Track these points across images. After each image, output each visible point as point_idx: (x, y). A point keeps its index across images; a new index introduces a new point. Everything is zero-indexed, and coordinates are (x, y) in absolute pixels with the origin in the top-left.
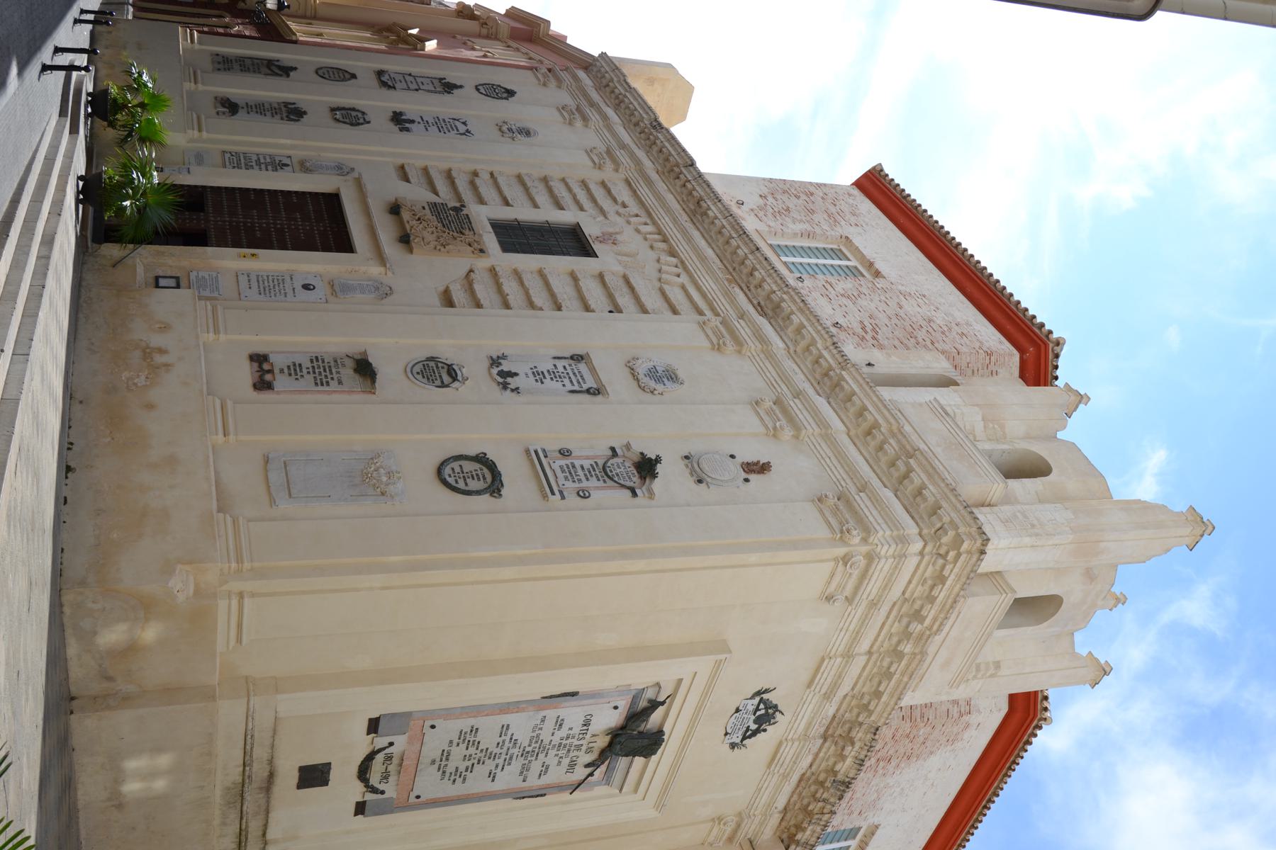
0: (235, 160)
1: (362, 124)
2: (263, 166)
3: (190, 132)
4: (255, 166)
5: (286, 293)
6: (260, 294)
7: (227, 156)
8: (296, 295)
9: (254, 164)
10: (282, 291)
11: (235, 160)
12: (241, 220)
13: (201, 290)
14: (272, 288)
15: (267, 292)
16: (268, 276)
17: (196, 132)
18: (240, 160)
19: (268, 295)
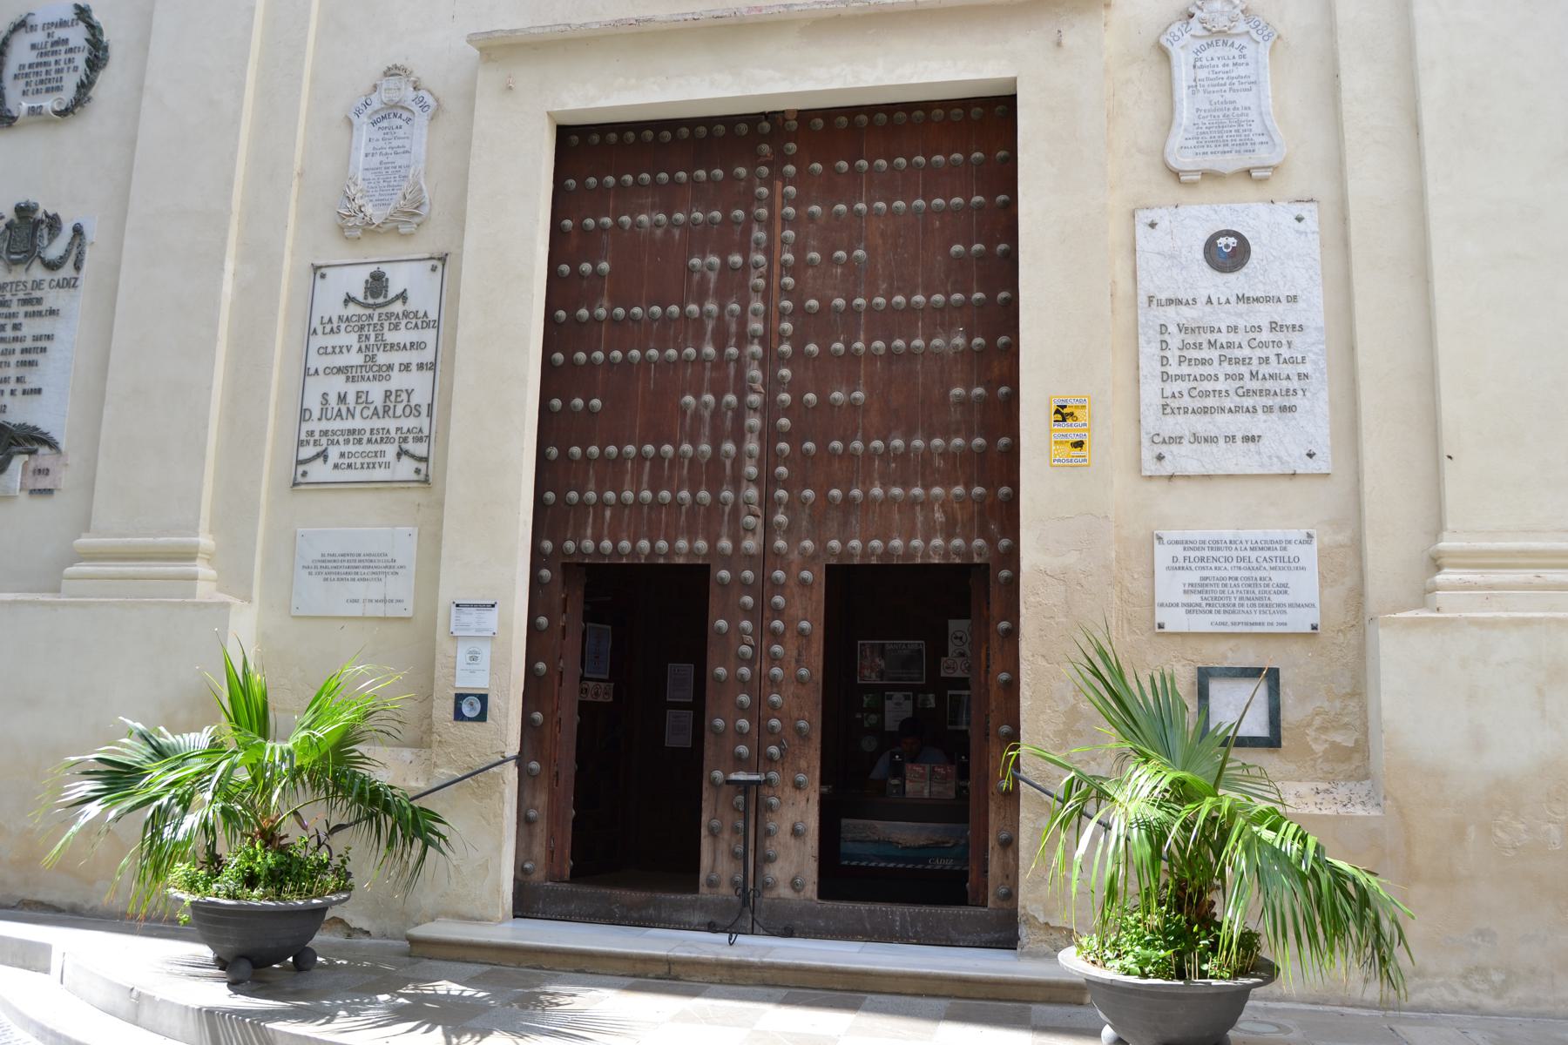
0: (352, 448)
1: (93, 28)
2: (383, 358)
3: (206, 590)
4: (393, 385)
5: (1274, 326)
6: (1292, 409)
7: (318, 471)
8: (1284, 292)
9: (376, 391)
10: (1265, 336)
11: (352, 448)
12: (753, 446)
13: (1276, 599)
14: (1244, 370)
15: (1269, 384)
16: (1165, 377)
17: (201, 568)
18: (352, 432)
19: (1295, 384)
